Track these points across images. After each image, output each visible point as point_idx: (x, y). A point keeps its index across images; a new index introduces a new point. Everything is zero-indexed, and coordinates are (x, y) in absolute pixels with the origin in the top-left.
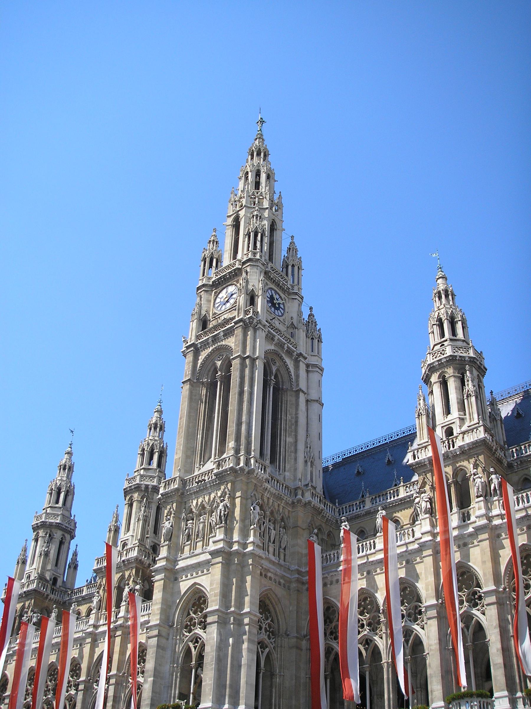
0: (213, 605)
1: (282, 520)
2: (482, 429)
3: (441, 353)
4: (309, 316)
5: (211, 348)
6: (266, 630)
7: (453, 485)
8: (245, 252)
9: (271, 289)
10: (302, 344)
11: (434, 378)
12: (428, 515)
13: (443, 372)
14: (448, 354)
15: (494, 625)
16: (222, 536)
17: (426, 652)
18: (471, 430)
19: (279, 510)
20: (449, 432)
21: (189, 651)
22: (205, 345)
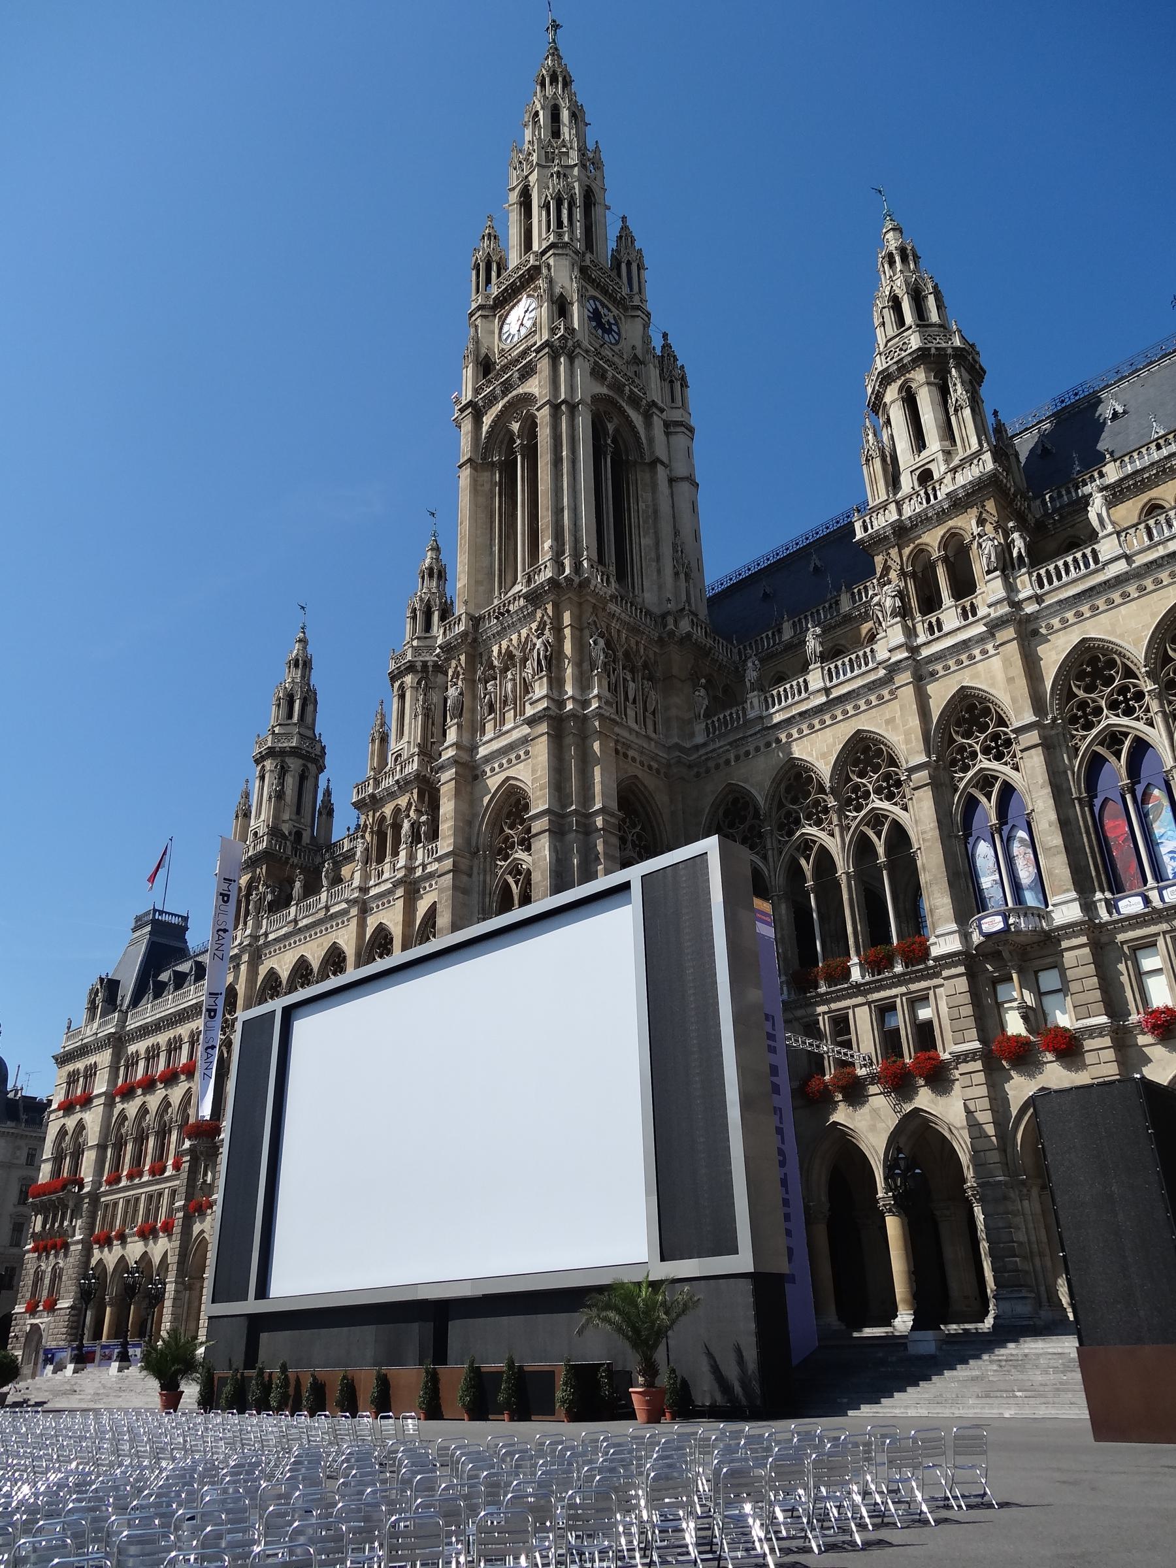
0: (539, 803)
1: (645, 666)
2: (987, 457)
3: (901, 350)
4: (663, 347)
5: (501, 404)
6: (634, 845)
7: (940, 563)
8: (544, 236)
9: (594, 298)
10: (655, 390)
11: (891, 393)
12: (898, 619)
13: (906, 382)
14: (914, 348)
15: (1041, 781)
16: (544, 692)
17: (916, 846)
18: (969, 461)
19: (638, 651)
20: (925, 477)
21: (507, 886)
22: (491, 400)
